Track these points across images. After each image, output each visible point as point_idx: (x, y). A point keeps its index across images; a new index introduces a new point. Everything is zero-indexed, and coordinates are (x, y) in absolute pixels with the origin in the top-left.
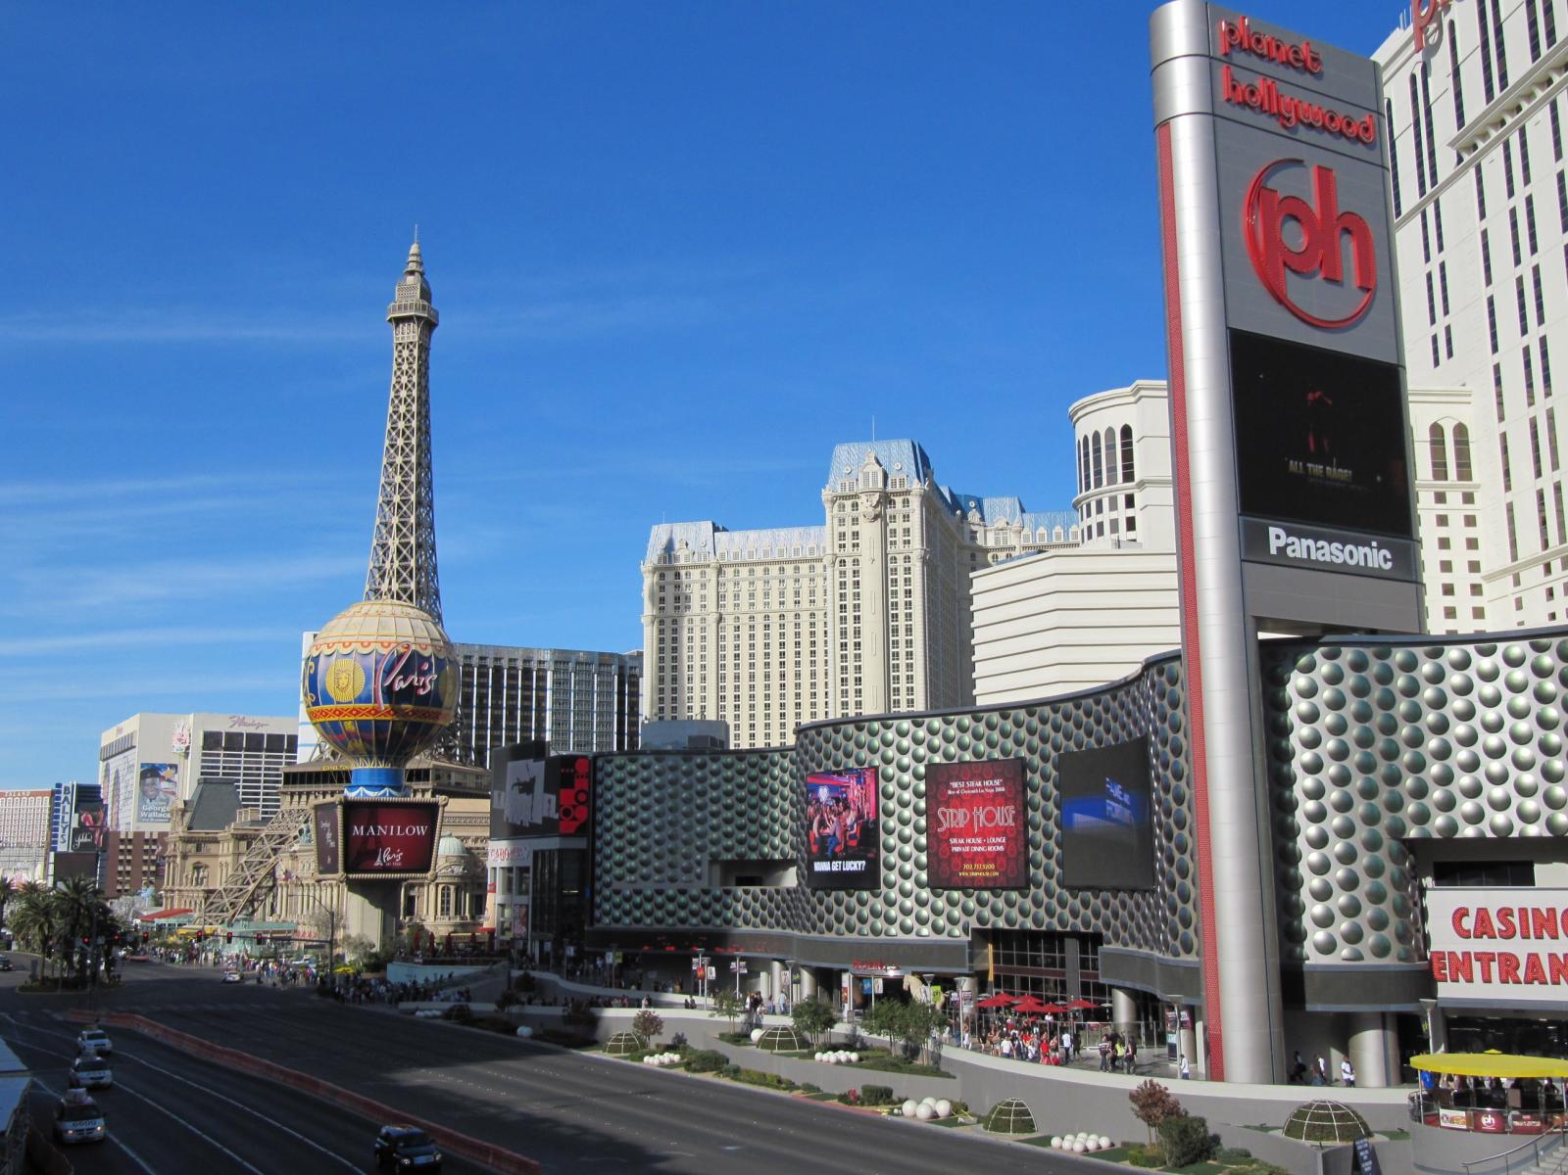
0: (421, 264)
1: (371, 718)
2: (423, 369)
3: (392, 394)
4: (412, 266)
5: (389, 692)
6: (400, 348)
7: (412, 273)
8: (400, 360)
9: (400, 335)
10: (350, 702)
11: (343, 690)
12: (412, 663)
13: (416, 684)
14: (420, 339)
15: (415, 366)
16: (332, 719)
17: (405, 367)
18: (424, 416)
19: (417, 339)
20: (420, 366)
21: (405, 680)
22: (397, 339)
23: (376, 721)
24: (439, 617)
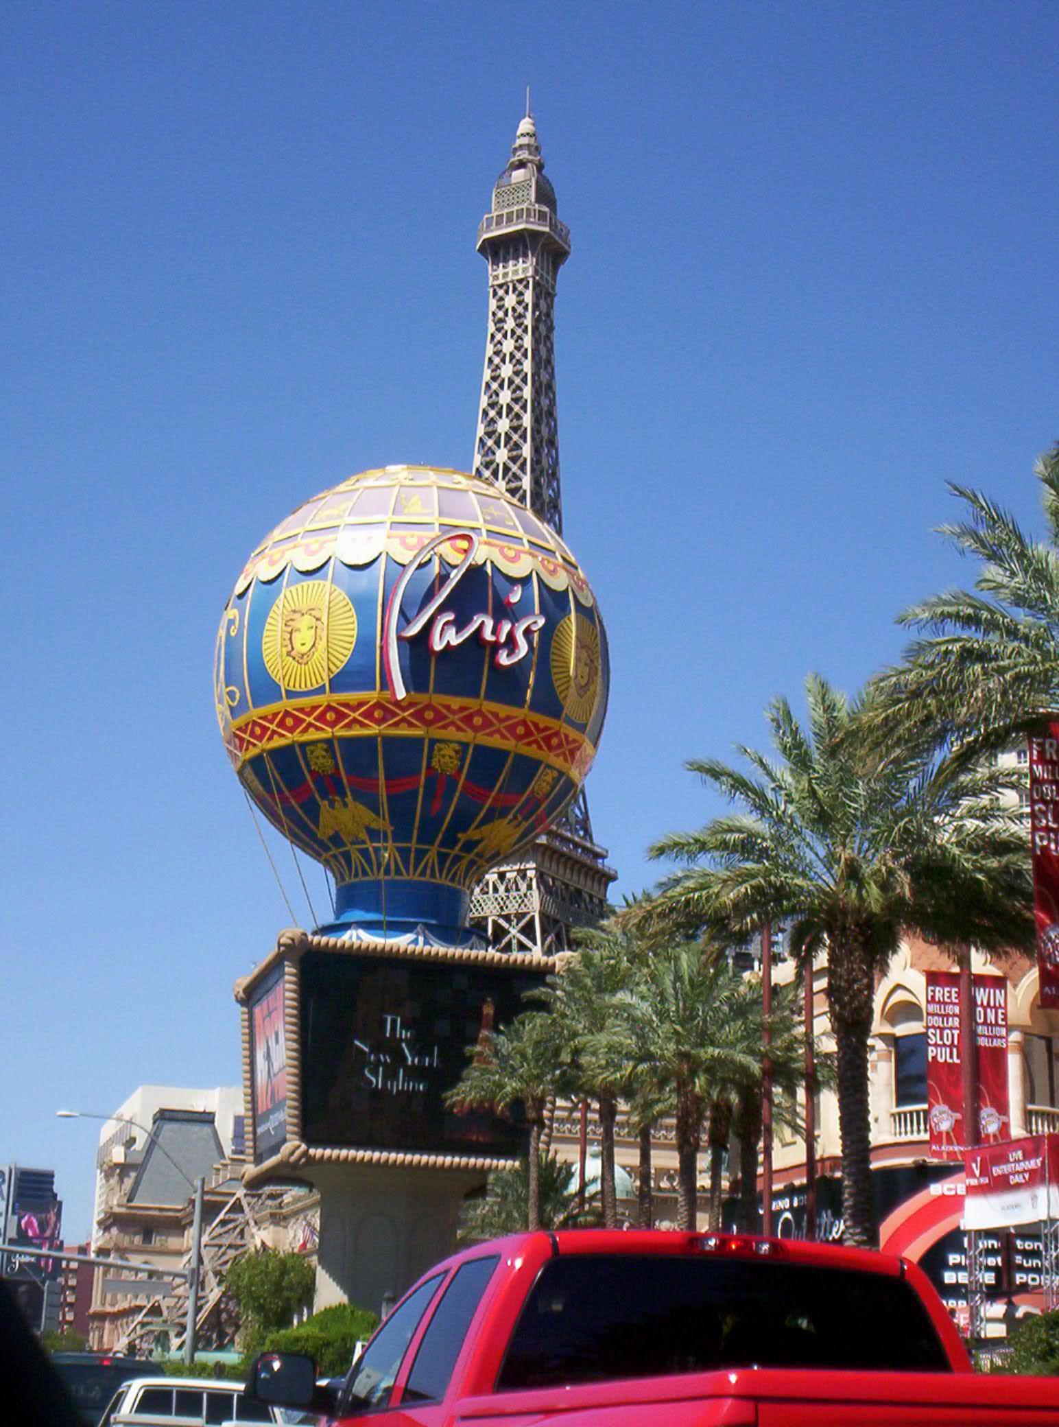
0: (537, 150)
1: (373, 730)
2: (542, 328)
3: (487, 374)
4: (524, 155)
5: (417, 646)
6: (501, 292)
7: (522, 165)
8: (500, 314)
9: (501, 271)
10: (321, 690)
11: (302, 659)
12: (475, 591)
13: (488, 635)
14: (536, 271)
15: (528, 321)
16: (277, 742)
17: (510, 324)
18: (545, 415)
19: (530, 272)
20: (537, 321)
21: (460, 624)
22: (496, 277)
23: (388, 740)
24: (555, 506)
